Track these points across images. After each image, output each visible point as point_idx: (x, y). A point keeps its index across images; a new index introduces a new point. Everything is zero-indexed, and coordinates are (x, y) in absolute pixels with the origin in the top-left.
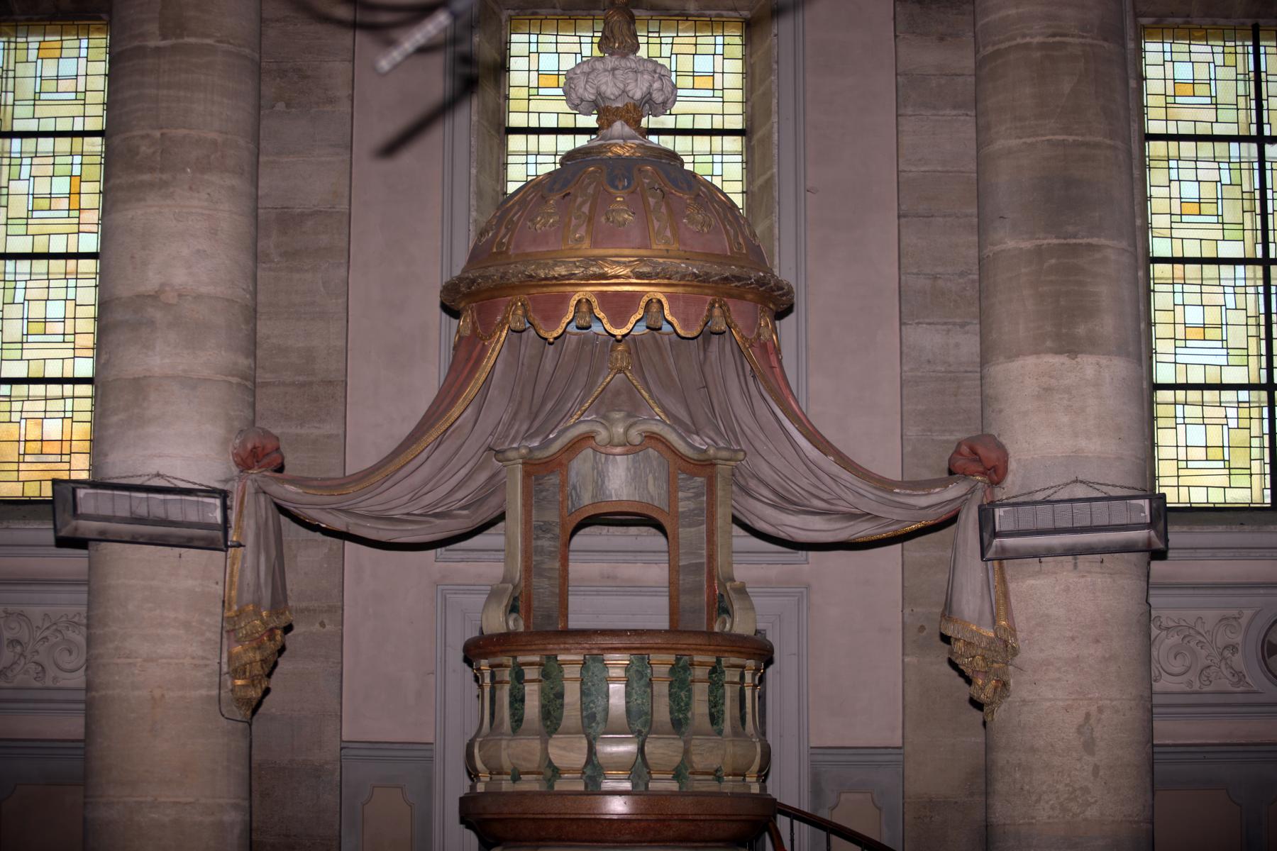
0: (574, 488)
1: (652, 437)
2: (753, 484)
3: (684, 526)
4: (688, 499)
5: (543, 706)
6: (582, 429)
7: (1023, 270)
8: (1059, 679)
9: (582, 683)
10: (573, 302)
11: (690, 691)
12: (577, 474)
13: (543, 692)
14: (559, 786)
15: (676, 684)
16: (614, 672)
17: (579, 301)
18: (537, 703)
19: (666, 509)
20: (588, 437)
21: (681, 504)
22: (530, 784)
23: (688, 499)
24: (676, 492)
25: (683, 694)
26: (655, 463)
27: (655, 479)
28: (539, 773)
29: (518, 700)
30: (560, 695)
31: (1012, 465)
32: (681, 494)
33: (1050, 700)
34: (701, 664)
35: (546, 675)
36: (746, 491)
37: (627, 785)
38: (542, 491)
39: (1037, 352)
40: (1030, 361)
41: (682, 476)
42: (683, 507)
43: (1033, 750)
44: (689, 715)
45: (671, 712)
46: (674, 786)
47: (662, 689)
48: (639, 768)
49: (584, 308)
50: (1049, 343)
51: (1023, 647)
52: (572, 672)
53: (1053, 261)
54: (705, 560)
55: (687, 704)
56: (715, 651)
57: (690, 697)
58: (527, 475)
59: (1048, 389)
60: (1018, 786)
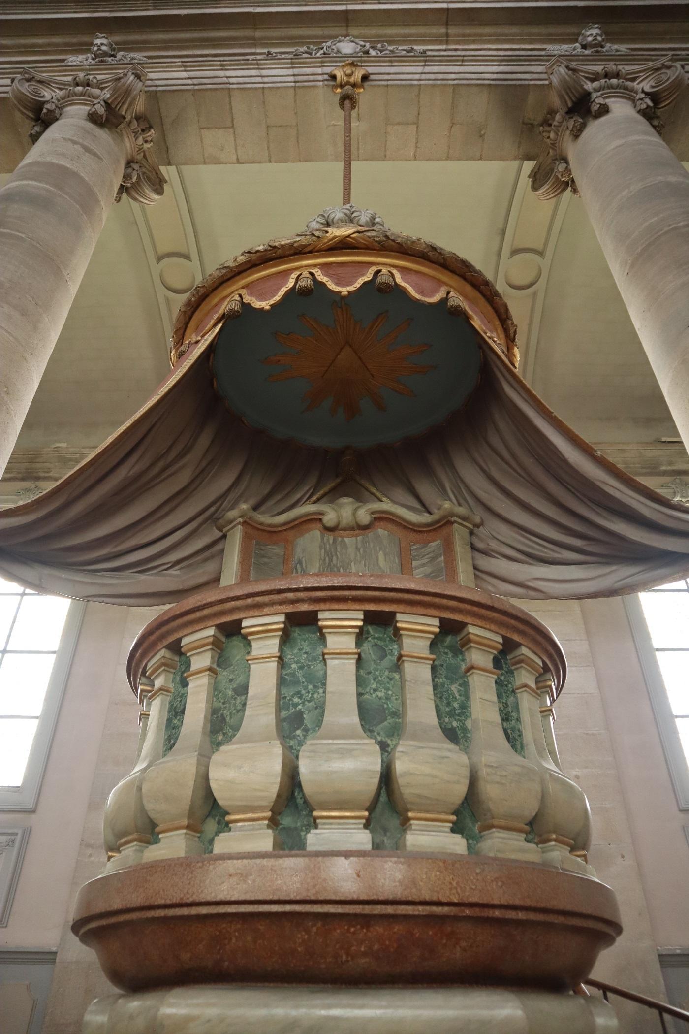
0: (300, 562)
1: (381, 518)
11: (465, 685)
12: (304, 550)
13: (215, 690)
16: (334, 642)
18: (203, 705)
20: (315, 519)
23: (424, 565)
25: (454, 688)
27: (385, 555)
34: (484, 645)
36: (485, 553)
38: (263, 557)
44: (469, 723)
45: (439, 717)
46: (457, 844)
47: (418, 675)
55: (464, 706)
56: (501, 624)
57: (467, 695)
58: (246, 537)
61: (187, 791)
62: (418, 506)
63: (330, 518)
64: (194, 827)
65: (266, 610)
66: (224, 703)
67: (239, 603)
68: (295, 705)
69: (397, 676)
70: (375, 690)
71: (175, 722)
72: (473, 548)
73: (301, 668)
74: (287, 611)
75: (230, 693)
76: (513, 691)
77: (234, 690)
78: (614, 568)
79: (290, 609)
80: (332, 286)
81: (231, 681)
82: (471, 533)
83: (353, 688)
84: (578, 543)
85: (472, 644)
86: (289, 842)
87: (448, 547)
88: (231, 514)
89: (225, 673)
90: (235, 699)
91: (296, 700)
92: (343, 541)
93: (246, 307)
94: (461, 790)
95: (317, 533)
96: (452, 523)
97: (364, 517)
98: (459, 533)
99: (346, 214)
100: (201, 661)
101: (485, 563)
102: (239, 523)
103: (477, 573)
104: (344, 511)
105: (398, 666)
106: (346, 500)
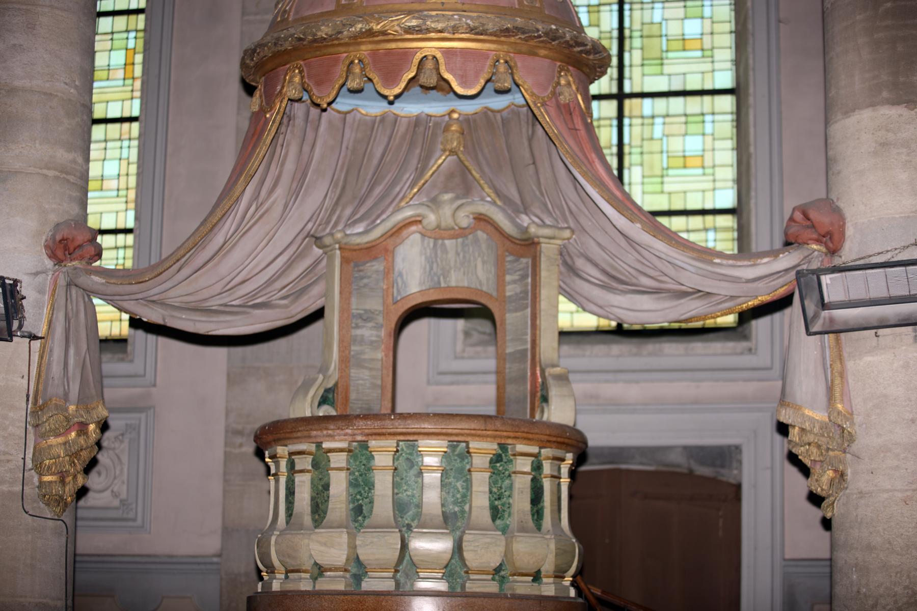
0: (401, 275)
2: (580, 263)
3: (510, 311)
4: (514, 282)
5: (313, 499)
6: (408, 213)
7: (858, 17)
8: (897, 467)
12: (403, 260)
14: (368, 585)
15: (466, 472)
19: (494, 294)
21: (508, 288)
22: (335, 583)
23: (514, 282)
24: (504, 275)
26: (484, 246)
27: (484, 262)
28: (346, 570)
31: (850, 231)
32: (508, 278)
33: (887, 491)
34: (480, 452)
35: (315, 465)
37: (442, 586)
38: (362, 278)
39: (872, 105)
40: (866, 115)
41: (509, 258)
43: (870, 548)
44: (467, 508)
48: (455, 566)
50: (885, 94)
51: (858, 430)
52: (338, 460)
53: (889, 5)
54: (529, 346)
56: (495, 437)
58: (345, 261)
59: (884, 145)
60: (855, 589)
68: (358, 500)
70: (406, 491)
73: (361, 475)
76: (510, 476)
77: (323, 486)
81: (320, 479)
83: (390, 492)
91: (358, 497)
92: (443, 245)
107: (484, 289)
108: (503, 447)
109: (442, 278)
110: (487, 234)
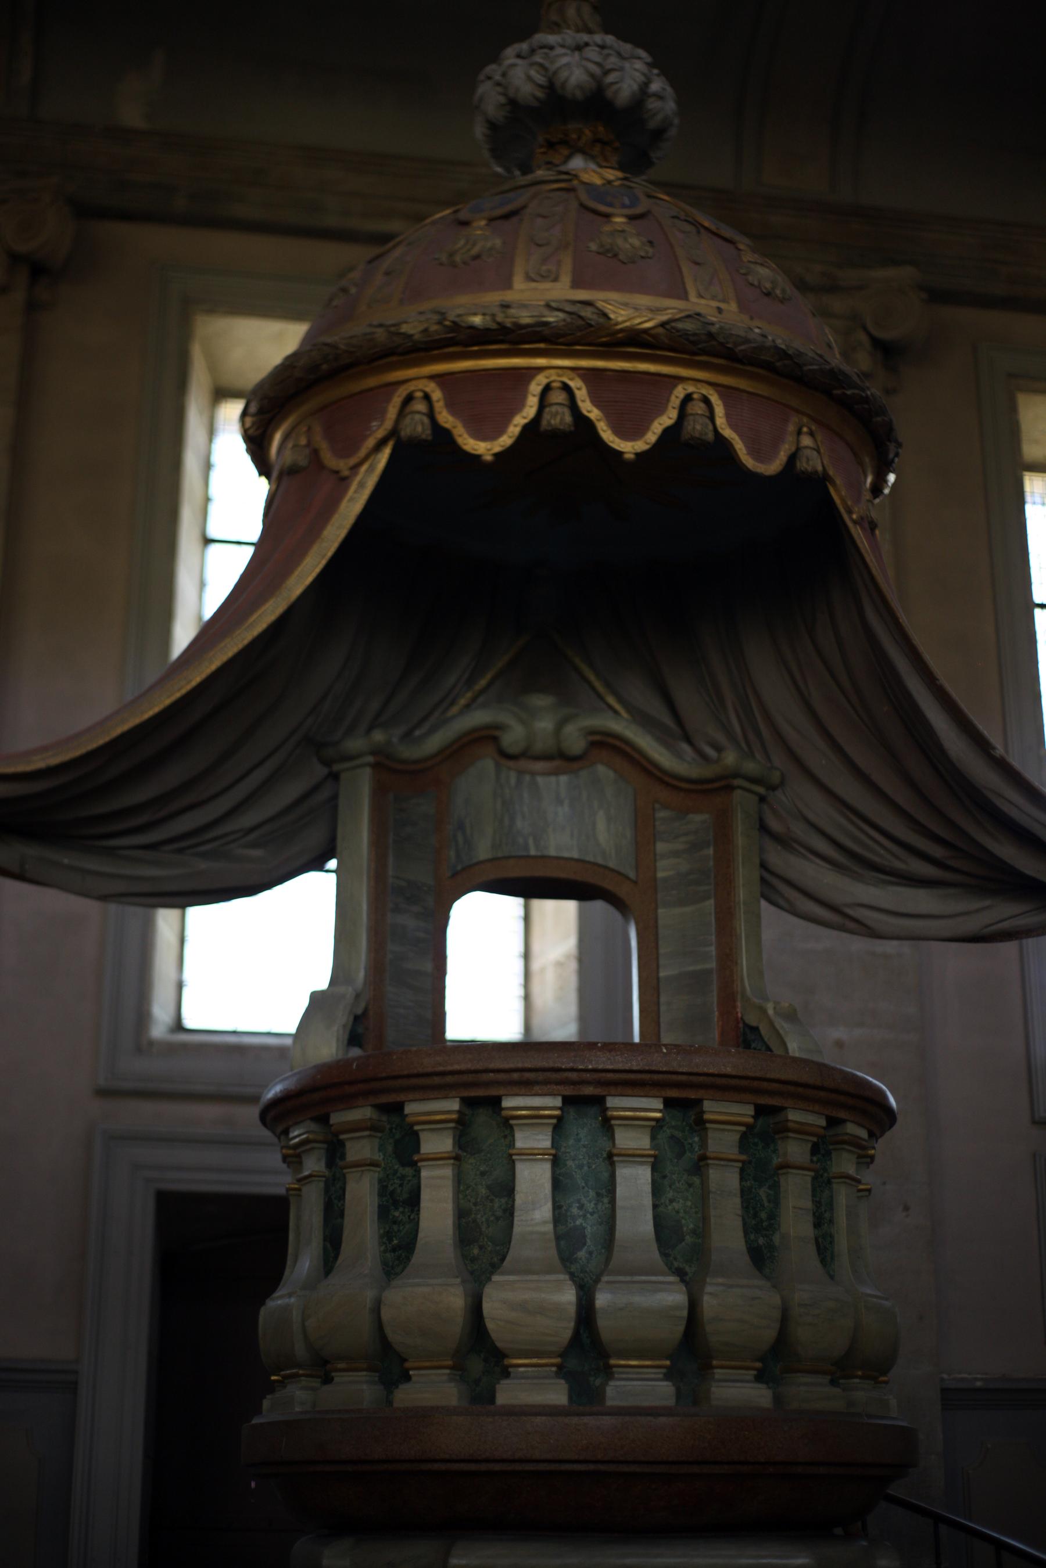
0: (461, 827)
1: (605, 744)
4: (676, 854)
6: (479, 718)
9: (556, 1162)
10: (535, 387)
11: (776, 1186)
16: (627, 1139)
17: (547, 389)
18: (449, 1207)
19: (632, 875)
20: (486, 737)
21: (661, 864)
23: (676, 854)
25: (763, 1193)
29: (400, 1203)
30: (508, 1189)
32: (661, 847)
34: (802, 1130)
36: (785, 842)
41: (661, 814)
42: (665, 870)
44: (776, 1239)
45: (746, 1233)
47: (725, 1180)
49: (558, 397)
54: (713, 965)
55: (773, 1216)
58: (379, 791)
61: (456, 1327)
62: (668, 721)
63: (514, 736)
64: (459, 1368)
65: (537, 1088)
66: (475, 1204)
67: (501, 1077)
69: (696, 1180)
70: (671, 1201)
71: (397, 1214)
72: (763, 828)
73: (580, 1167)
74: (566, 1093)
75: (483, 1191)
76: (829, 1182)
77: (488, 1187)
78: (987, 903)
79: (569, 1091)
80: (607, 435)
81: (483, 1174)
82: (762, 799)
83: (648, 1201)
84: (937, 851)
85: (790, 1134)
86: (586, 1394)
87: (722, 832)
88: (355, 744)
89: (472, 1161)
90: (492, 1201)
93: (443, 436)
94: (770, 1334)
95: (488, 765)
96: (730, 788)
97: (574, 739)
98: (742, 802)
99: (592, 75)
100: (437, 1143)
101: (777, 858)
102: (369, 765)
103: (767, 876)
104: (537, 721)
105: (700, 1165)
106: (541, 701)
107: (611, 864)
108: (833, 1122)
109: (531, 841)
110: (615, 771)
